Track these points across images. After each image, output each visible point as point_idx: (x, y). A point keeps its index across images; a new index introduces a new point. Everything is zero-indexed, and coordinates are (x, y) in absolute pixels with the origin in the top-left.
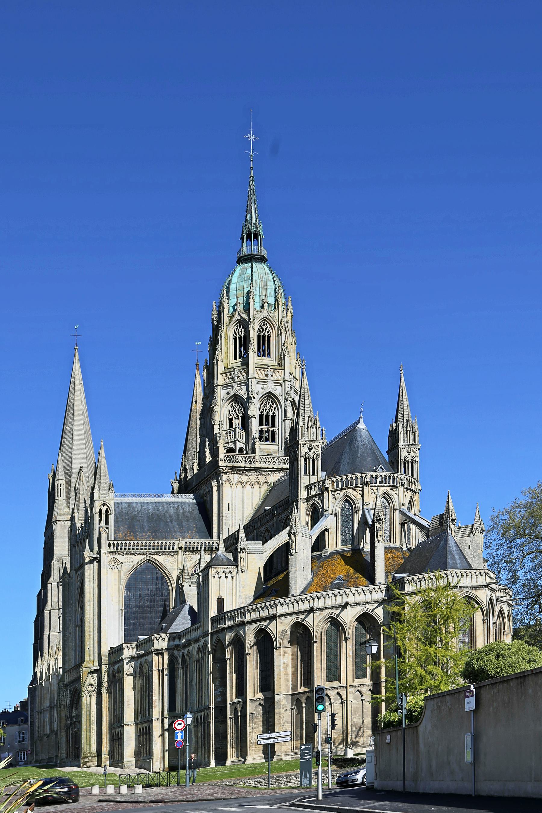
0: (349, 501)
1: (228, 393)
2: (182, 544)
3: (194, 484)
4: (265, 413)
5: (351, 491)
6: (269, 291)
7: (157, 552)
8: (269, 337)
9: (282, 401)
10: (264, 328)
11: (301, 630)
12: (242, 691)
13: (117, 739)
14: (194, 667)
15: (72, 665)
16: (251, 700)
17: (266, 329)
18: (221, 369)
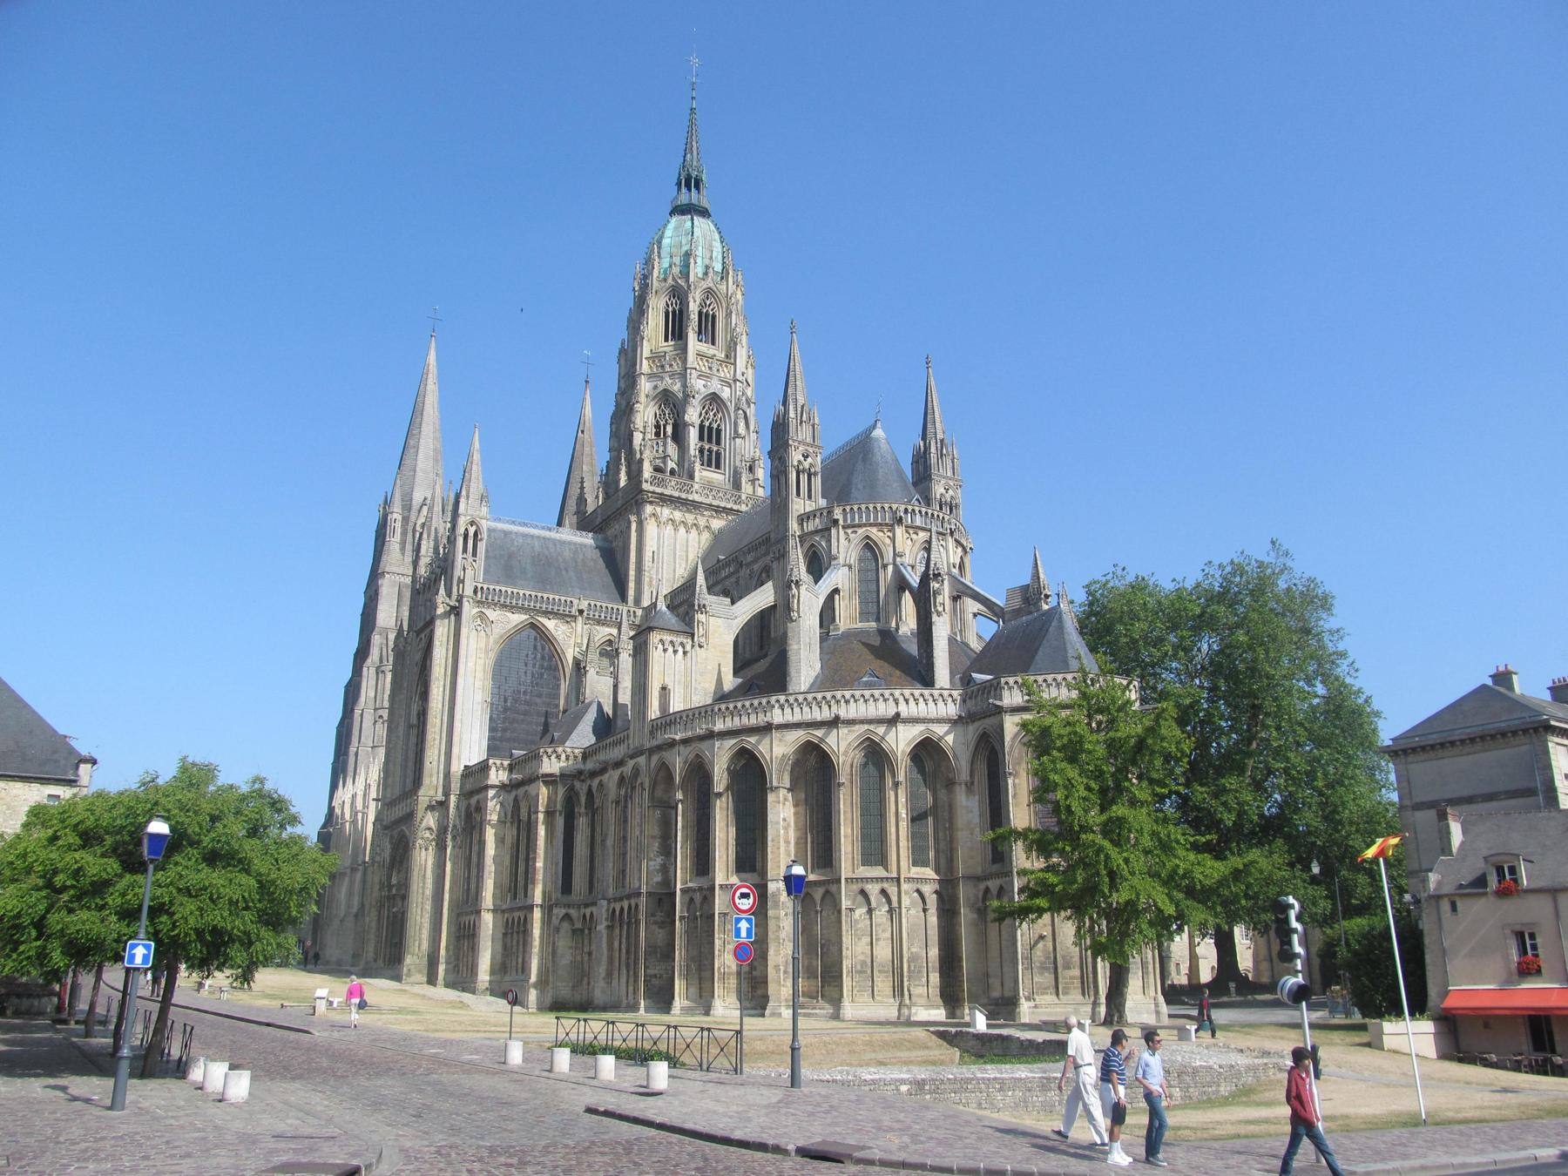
0: (870, 547)
1: (656, 387)
2: (584, 605)
3: (599, 520)
5: (874, 530)
7: (547, 613)
8: (714, 317)
9: (732, 409)
11: (812, 760)
12: (703, 863)
13: (465, 935)
14: (611, 814)
15: (397, 792)
18: (646, 353)
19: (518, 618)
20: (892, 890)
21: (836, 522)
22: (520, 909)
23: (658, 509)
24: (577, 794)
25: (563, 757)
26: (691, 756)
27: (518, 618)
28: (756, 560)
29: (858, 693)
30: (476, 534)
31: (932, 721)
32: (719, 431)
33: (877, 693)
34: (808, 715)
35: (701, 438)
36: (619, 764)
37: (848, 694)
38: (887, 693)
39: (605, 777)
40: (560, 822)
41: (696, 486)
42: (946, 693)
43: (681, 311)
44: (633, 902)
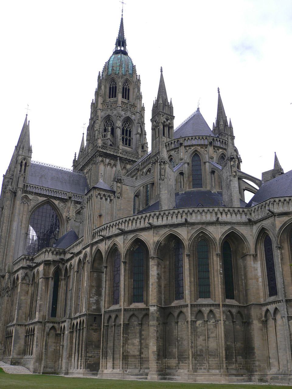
4: (125, 128)
5: (199, 148)
6: (129, 67)
7: (55, 198)
8: (129, 90)
10: (126, 84)
16: (125, 310)
17: (127, 86)
19: (41, 199)
20: (216, 310)
21: (181, 144)
22: (32, 324)
23: (104, 159)
24: (61, 270)
25: (55, 253)
26: (112, 245)
27: (41, 199)
28: (145, 167)
29: (196, 210)
30: (26, 163)
31: (234, 223)
32: (130, 132)
33: (206, 209)
34: (170, 221)
35: (123, 133)
36: (80, 253)
37: (191, 210)
38: (211, 209)
39: (73, 261)
40: (51, 283)
41: (120, 151)
42: (241, 210)
43: (116, 87)
44: (82, 319)
